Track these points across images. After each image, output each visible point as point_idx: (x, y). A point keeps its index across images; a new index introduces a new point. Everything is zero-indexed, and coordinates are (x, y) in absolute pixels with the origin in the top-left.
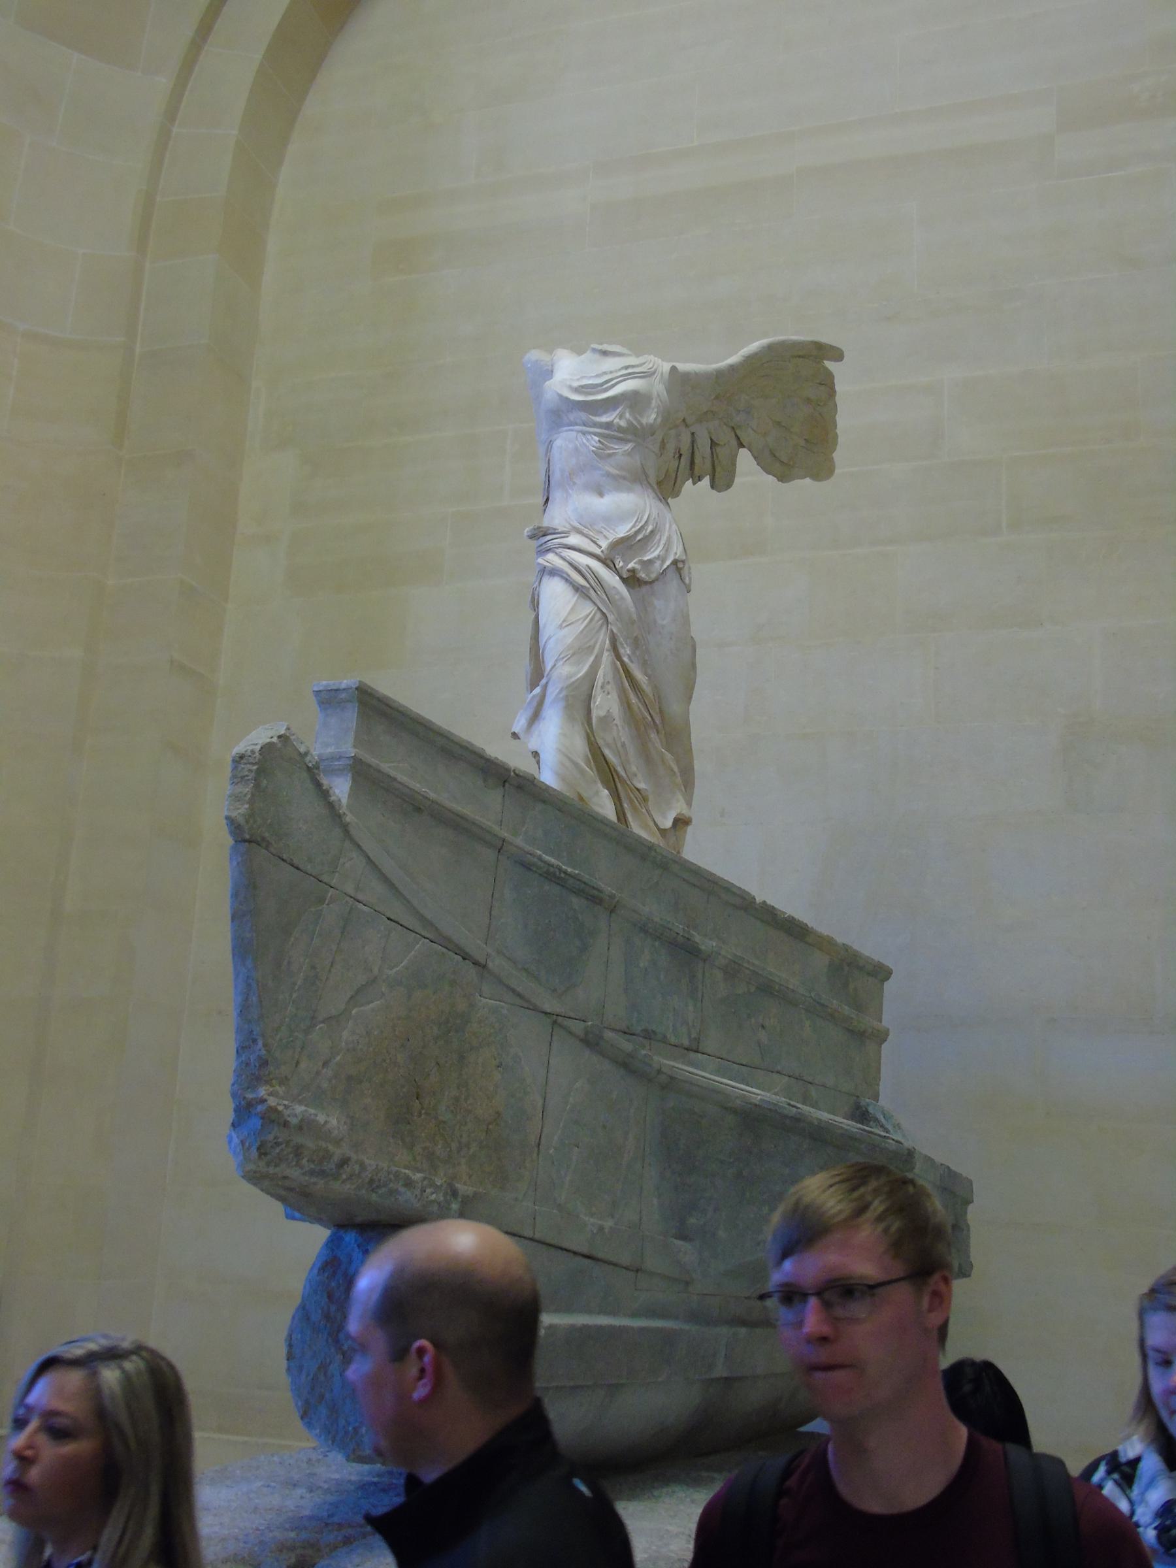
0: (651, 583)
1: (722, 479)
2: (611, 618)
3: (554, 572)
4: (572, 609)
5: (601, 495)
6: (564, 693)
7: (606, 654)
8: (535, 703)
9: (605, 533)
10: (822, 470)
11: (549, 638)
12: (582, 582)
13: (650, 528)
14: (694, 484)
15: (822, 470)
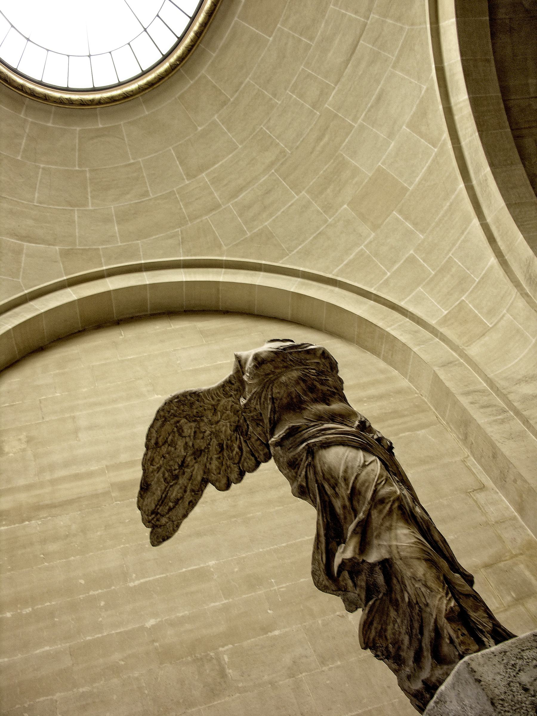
3: (326, 445)
6: (396, 505)
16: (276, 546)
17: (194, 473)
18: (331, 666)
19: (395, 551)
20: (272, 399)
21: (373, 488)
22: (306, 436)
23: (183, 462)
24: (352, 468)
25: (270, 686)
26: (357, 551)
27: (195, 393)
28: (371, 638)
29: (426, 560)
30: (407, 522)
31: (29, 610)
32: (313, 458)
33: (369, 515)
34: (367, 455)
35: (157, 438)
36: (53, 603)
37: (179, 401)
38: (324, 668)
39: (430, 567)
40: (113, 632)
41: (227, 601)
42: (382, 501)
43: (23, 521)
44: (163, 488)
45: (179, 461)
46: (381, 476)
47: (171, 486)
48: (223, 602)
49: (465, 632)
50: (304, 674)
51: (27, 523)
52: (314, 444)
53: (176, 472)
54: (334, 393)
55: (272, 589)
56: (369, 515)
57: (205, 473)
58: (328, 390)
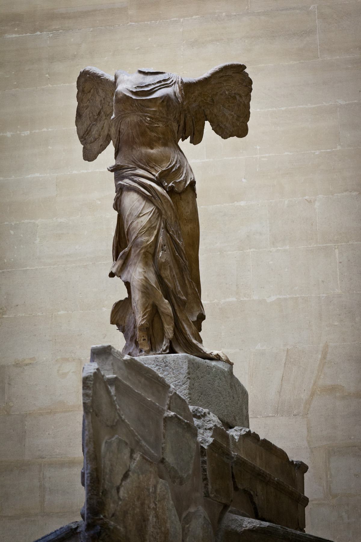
0: (180, 194)
1: (197, 139)
2: (163, 212)
3: (130, 189)
4: (143, 207)
5: (152, 148)
6: (143, 251)
7: (162, 230)
8: (124, 257)
9: (156, 168)
10: (242, 132)
11: (133, 222)
12: (148, 194)
13: (178, 166)
14: (183, 140)
15: (242, 132)
16: (275, 109)
17: (105, 125)
18: (279, 248)
19: (132, 280)
20: (119, 131)
21: (135, 235)
22: (124, 174)
23: (99, 113)
24: (132, 215)
25: (219, 253)
26: (119, 269)
27: (99, 77)
28: (116, 319)
29: (142, 292)
30: (146, 264)
31: (27, 133)
32: (121, 194)
33: (130, 250)
34: (148, 204)
35: (83, 88)
36: (50, 130)
37: (89, 77)
38: (272, 249)
39: (143, 297)
40: (97, 170)
41: (208, 160)
42: (137, 246)
43: (35, 31)
44: (88, 124)
45: (98, 111)
46: (144, 227)
47: (93, 125)
48: (204, 161)
49: (146, 339)
50: (252, 250)
51: (38, 33)
52: (124, 185)
53: (96, 117)
54: (159, 139)
55: (254, 156)
56: (130, 250)
57: (109, 130)
58: (155, 136)
